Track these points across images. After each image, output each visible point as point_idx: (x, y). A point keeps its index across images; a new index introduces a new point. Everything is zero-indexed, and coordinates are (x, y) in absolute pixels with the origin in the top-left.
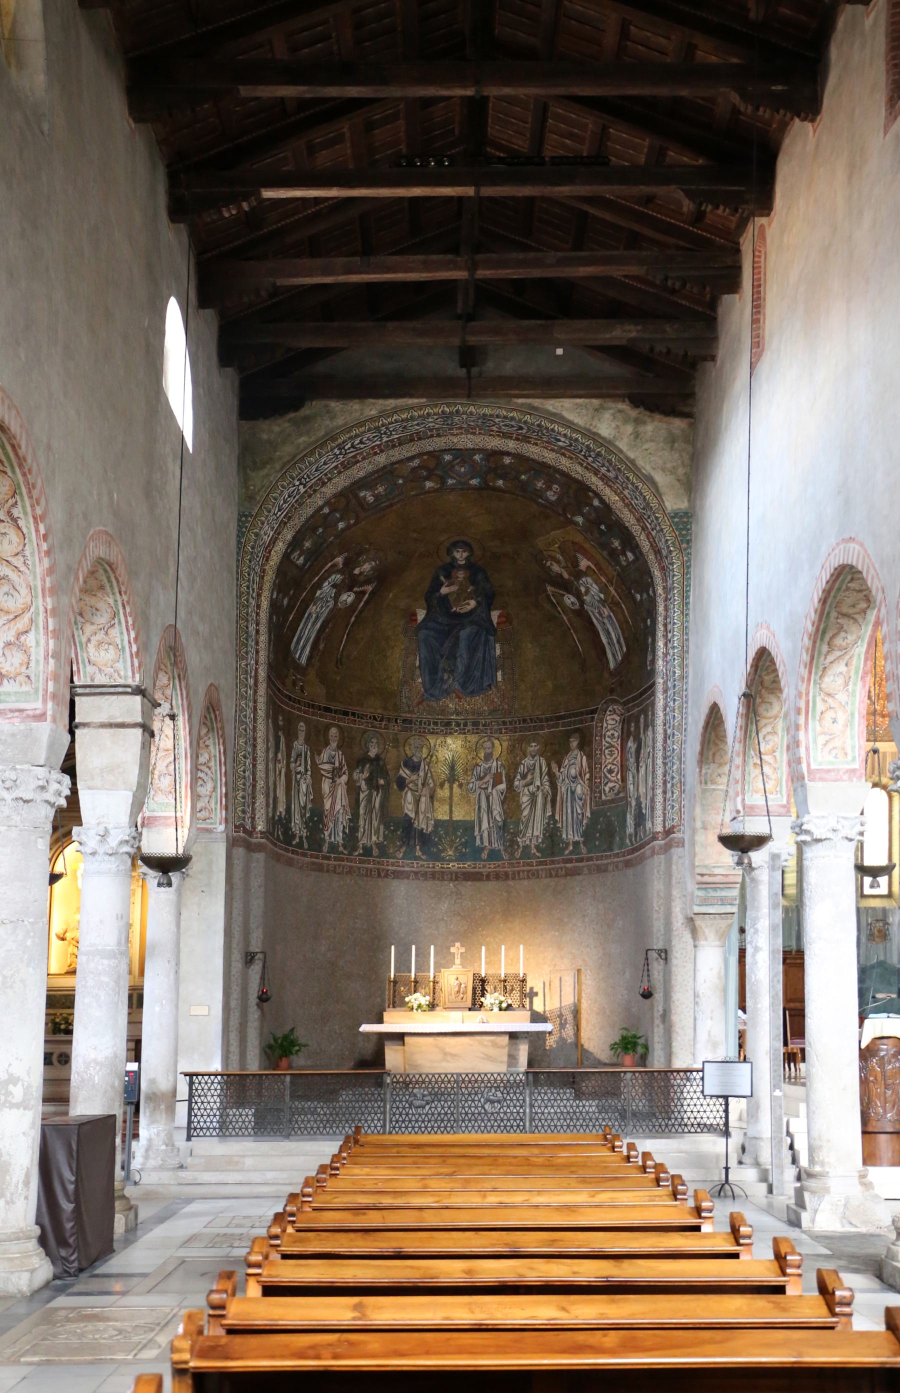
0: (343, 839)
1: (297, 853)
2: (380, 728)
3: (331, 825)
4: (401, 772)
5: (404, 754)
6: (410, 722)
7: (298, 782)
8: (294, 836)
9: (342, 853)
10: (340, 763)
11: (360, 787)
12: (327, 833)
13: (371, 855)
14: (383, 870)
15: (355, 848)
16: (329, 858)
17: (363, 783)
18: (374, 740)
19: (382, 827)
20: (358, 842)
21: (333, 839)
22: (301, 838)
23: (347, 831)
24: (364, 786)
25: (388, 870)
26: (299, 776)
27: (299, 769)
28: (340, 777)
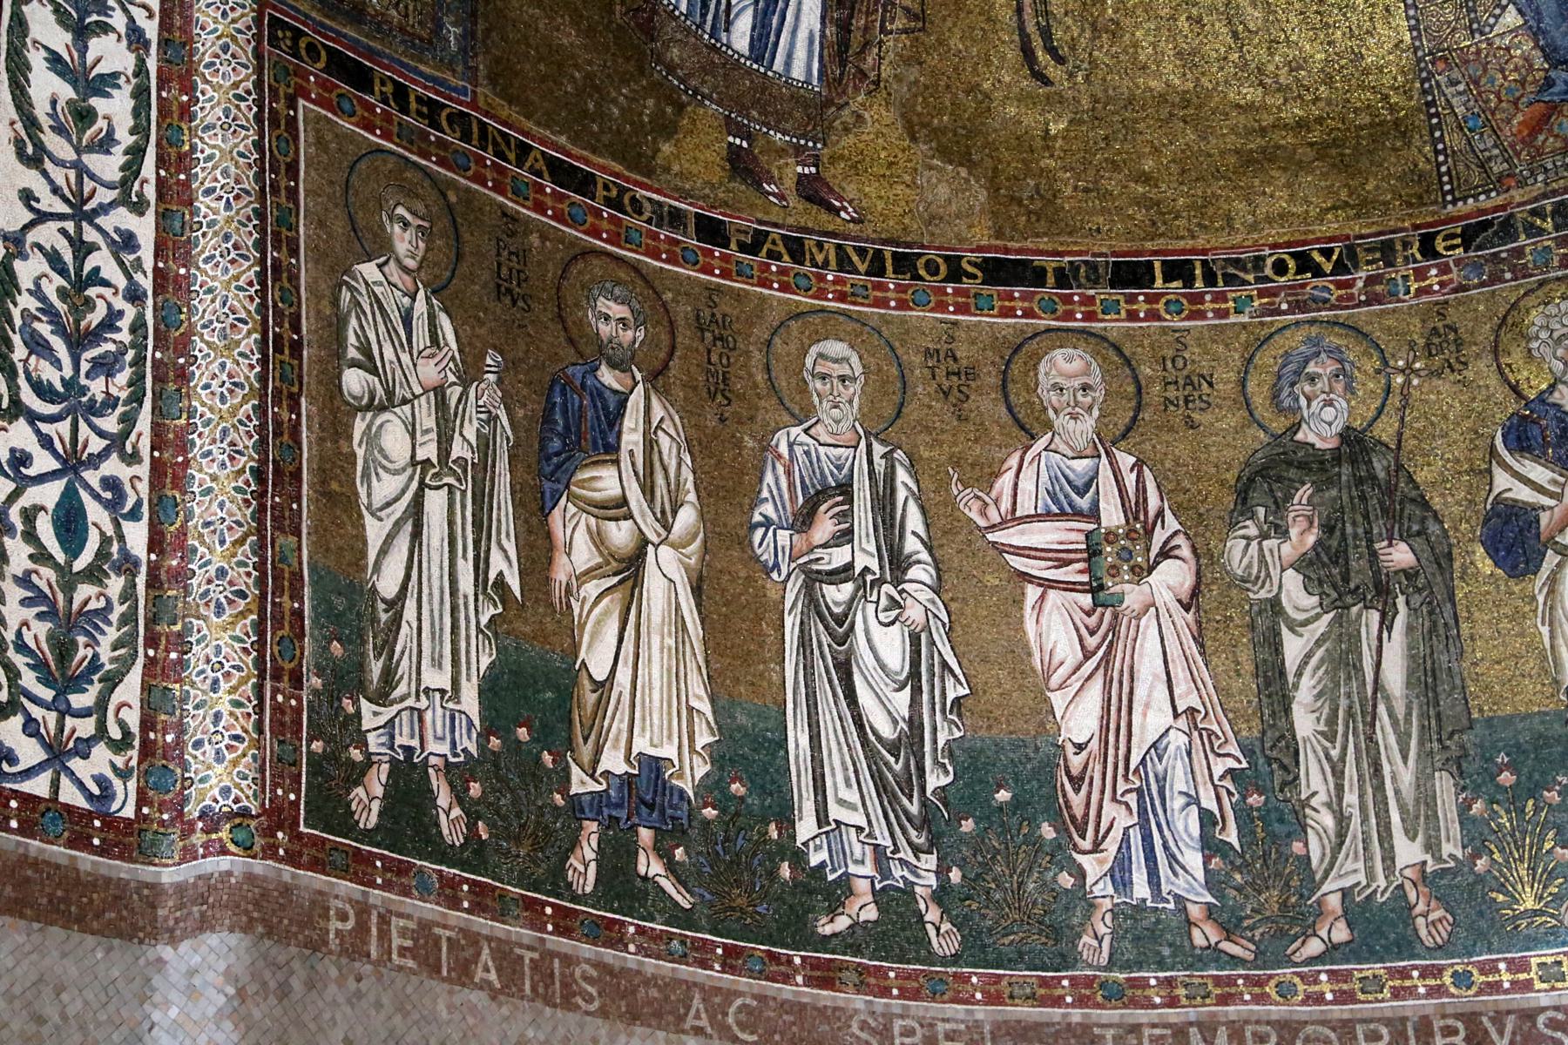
0: (1213, 882)
1: (876, 985)
2: (1347, 302)
3: (1119, 818)
4: (1502, 480)
5: (1501, 393)
6: (1507, 230)
7: (841, 626)
8: (838, 894)
9: (1214, 955)
10: (1134, 509)
11: (1275, 604)
12: (1093, 866)
13: (1407, 945)
14: (1499, 1018)
15: (1303, 919)
16: (1116, 995)
17: (1292, 580)
18: (1323, 367)
19: (1444, 785)
20: (1311, 883)
21: (1141, 890)
22: (894, 900)
23: (1232, 836)
24: (1295, 594)
25: (1529, 1015)
26: (837, 594)
27: (839, 557)
28: (1141, 573)
